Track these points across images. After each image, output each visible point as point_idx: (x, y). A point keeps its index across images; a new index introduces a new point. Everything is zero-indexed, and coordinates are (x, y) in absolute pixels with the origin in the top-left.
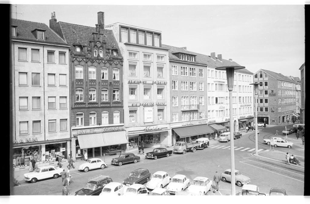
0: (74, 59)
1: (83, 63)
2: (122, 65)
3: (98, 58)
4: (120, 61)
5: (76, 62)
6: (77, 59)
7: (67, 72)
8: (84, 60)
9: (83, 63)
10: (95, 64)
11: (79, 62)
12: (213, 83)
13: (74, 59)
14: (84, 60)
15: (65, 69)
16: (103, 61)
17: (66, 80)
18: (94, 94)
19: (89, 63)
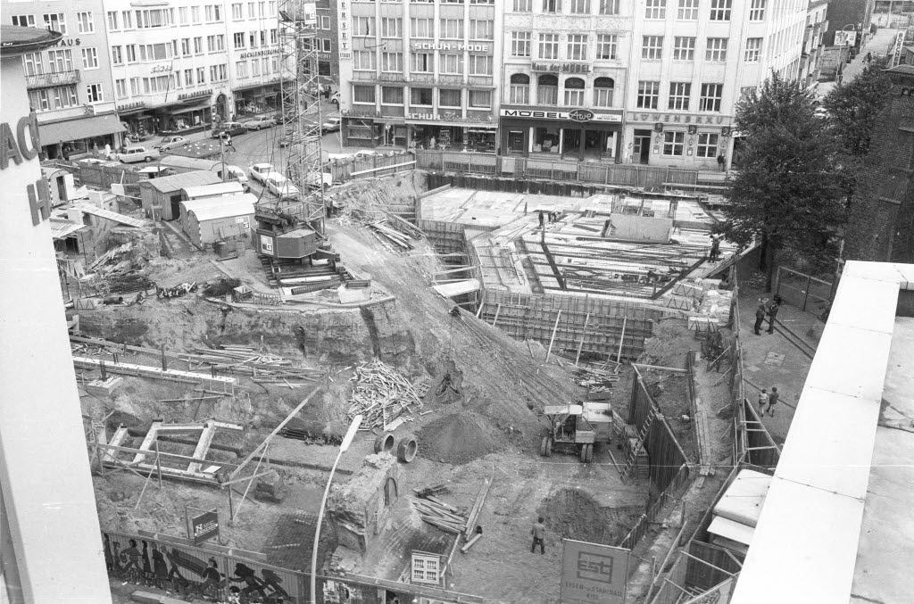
12: (128, 8)
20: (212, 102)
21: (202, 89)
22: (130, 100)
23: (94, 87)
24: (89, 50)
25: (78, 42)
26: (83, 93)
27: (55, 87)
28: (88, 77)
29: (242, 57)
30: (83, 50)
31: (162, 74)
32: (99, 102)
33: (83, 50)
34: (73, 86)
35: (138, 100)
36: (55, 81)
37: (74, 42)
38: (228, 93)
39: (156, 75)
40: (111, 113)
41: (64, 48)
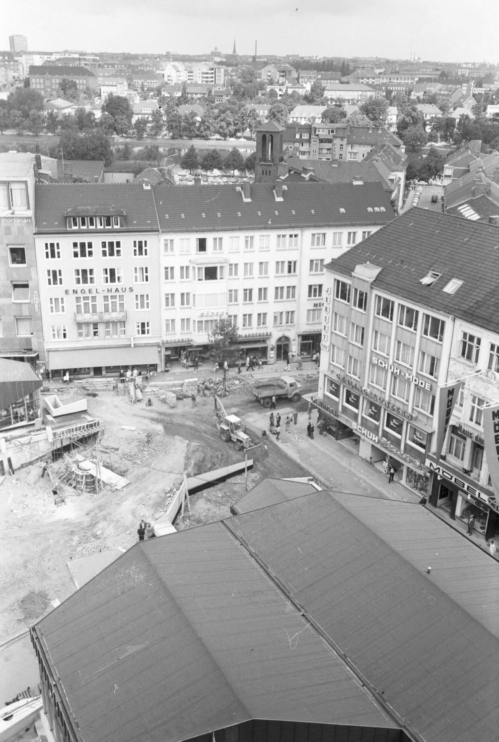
20: (272, 342)
21: (262, 331)
22: (178, 336)
23: (143, 324)
24: (142, 296)
25: (131, 290)
26: (132, 328)
27: (107, 323)
28: (136, 315)
29: (315, 305)
30: (137, 296)
31: (209, 319)
32: (146, 335)
33: (137, 296)
34: (123, 323)
35: (185, 337)
36: (106, 317)
37: (128, 290)
38: (292, 334)
39: (204, 319)
40: (152, 345)
41: (117, 294)
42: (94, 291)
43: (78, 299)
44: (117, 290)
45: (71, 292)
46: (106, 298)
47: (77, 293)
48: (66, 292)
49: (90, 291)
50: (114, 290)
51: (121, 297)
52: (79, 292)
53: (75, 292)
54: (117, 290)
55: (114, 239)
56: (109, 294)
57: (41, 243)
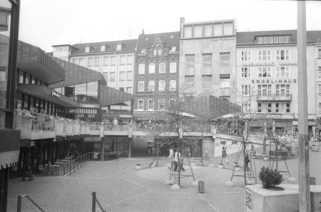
0: (138, 59)
1: (144, 61)
2: (179, 59)
3: (157, 56)
4: (176, 56)
5: (139, 62)
6: (140, 59)
7: (133, 70)
8: (145, 59)
9: (144, 61)
10: (155, 61)
11: (142, 61)
13: (138, 59)
14: (145, 59)
15: (131, 68)
16: (161, 58)
17: (132, 76)
18: (152, 83)
19: (149, 61)
36: (277, 99)
37: (293, 81)
42: (270, 81)
43: (259, 86)
44: (285, 81)
45: (255, 81)
46: (278, 86)
47: (259, 82)
48: (253, 81)
49: (268, 81)
50: (283, 81)
51: (288, 86)
52: (261, 81)
53: (258, 81)
54: (285, 81)
55: (284, 49)
56: (280, 84)
57: (239, 51)
